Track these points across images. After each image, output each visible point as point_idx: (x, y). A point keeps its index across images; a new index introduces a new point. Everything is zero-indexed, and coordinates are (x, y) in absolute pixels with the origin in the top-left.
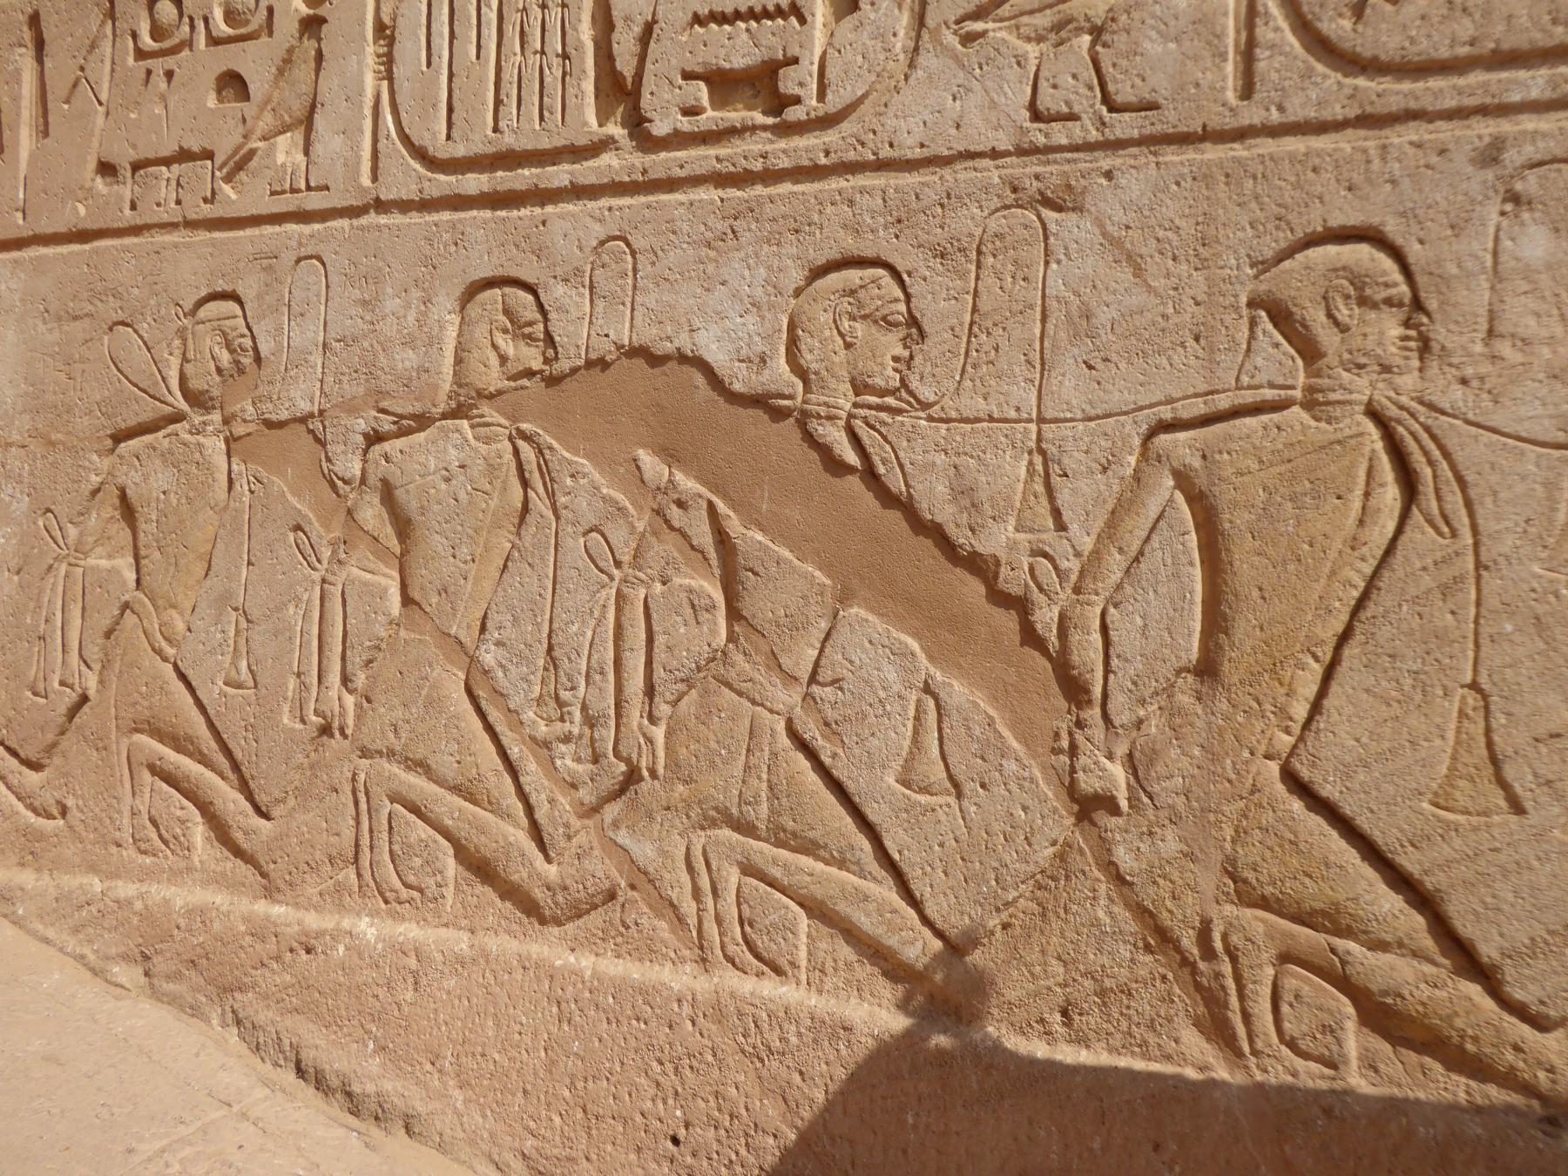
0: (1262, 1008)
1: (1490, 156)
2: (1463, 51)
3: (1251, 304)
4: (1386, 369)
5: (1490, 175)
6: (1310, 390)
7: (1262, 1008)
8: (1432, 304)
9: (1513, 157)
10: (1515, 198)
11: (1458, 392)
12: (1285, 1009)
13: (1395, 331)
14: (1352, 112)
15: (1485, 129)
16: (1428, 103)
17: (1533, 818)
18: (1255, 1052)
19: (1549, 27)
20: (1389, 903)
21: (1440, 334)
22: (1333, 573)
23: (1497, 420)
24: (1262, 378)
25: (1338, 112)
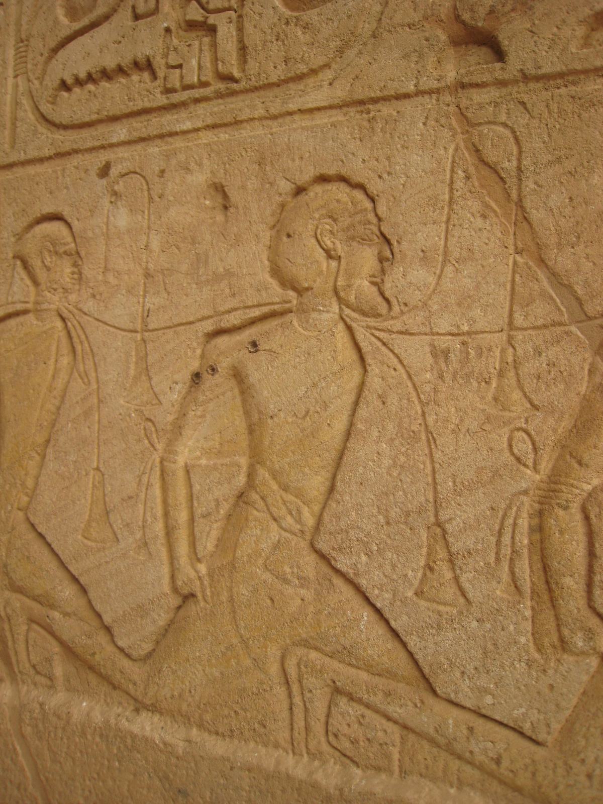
0: (21, 647)
1: (104, 171)
2: (94, 117)
3: (14, 257)
4: (65, 290)
5: (104, 182)
6: (37, 303)
7: (21, 647)
8: (83, 254)
9: (114, 172)
10: (115, 193)
11: (91, 303)
12: (30, 648)
13: (68, 270)
14: (52, 152)
15: (103, 157)
16: (80, 145)
17: (122, 545)
18: (20, 672)
19: (127, 102)
20: (67, 592)
21: (87, 271)
22: (42, 406)
23: (106, 317)
24: (16, 298)
25: (47, 152)
